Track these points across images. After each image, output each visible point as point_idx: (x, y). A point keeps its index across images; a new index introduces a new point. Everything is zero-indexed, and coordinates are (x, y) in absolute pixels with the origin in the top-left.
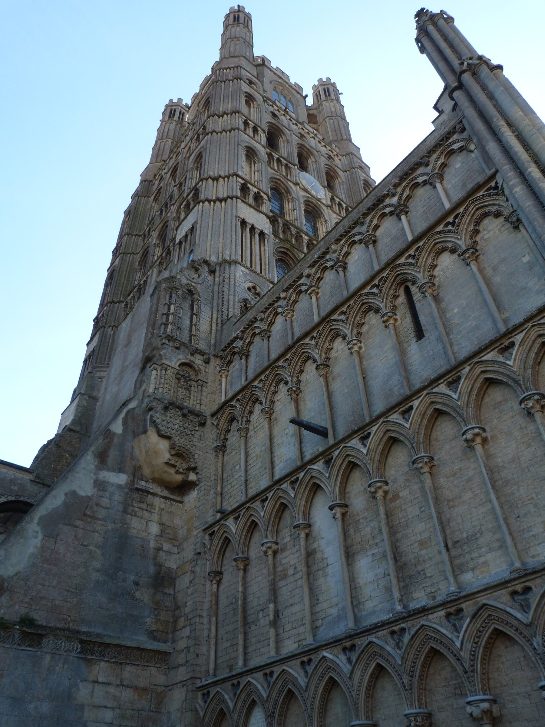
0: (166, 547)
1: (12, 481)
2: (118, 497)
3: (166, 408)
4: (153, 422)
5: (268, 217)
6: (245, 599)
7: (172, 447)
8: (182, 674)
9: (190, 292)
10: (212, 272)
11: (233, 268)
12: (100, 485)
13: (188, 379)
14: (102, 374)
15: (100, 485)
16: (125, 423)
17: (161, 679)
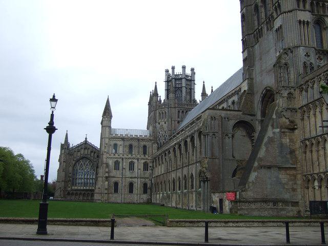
0: (291, 144)
1: (237, 115)
2: (278, 135)
3: (286, 111)
4: (284, 116)
5: (309, 11)
6: (312, 159)
7: (289, 120)
8: (300, 172)
9: (286, 65)
10: (292, 52)
11: (299, 49)
12: (274, 133)
13: (290, 97)
14: (253, 68)
15: (274, 133)
16: (276, 114)
17: (295, 172)
